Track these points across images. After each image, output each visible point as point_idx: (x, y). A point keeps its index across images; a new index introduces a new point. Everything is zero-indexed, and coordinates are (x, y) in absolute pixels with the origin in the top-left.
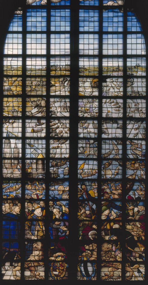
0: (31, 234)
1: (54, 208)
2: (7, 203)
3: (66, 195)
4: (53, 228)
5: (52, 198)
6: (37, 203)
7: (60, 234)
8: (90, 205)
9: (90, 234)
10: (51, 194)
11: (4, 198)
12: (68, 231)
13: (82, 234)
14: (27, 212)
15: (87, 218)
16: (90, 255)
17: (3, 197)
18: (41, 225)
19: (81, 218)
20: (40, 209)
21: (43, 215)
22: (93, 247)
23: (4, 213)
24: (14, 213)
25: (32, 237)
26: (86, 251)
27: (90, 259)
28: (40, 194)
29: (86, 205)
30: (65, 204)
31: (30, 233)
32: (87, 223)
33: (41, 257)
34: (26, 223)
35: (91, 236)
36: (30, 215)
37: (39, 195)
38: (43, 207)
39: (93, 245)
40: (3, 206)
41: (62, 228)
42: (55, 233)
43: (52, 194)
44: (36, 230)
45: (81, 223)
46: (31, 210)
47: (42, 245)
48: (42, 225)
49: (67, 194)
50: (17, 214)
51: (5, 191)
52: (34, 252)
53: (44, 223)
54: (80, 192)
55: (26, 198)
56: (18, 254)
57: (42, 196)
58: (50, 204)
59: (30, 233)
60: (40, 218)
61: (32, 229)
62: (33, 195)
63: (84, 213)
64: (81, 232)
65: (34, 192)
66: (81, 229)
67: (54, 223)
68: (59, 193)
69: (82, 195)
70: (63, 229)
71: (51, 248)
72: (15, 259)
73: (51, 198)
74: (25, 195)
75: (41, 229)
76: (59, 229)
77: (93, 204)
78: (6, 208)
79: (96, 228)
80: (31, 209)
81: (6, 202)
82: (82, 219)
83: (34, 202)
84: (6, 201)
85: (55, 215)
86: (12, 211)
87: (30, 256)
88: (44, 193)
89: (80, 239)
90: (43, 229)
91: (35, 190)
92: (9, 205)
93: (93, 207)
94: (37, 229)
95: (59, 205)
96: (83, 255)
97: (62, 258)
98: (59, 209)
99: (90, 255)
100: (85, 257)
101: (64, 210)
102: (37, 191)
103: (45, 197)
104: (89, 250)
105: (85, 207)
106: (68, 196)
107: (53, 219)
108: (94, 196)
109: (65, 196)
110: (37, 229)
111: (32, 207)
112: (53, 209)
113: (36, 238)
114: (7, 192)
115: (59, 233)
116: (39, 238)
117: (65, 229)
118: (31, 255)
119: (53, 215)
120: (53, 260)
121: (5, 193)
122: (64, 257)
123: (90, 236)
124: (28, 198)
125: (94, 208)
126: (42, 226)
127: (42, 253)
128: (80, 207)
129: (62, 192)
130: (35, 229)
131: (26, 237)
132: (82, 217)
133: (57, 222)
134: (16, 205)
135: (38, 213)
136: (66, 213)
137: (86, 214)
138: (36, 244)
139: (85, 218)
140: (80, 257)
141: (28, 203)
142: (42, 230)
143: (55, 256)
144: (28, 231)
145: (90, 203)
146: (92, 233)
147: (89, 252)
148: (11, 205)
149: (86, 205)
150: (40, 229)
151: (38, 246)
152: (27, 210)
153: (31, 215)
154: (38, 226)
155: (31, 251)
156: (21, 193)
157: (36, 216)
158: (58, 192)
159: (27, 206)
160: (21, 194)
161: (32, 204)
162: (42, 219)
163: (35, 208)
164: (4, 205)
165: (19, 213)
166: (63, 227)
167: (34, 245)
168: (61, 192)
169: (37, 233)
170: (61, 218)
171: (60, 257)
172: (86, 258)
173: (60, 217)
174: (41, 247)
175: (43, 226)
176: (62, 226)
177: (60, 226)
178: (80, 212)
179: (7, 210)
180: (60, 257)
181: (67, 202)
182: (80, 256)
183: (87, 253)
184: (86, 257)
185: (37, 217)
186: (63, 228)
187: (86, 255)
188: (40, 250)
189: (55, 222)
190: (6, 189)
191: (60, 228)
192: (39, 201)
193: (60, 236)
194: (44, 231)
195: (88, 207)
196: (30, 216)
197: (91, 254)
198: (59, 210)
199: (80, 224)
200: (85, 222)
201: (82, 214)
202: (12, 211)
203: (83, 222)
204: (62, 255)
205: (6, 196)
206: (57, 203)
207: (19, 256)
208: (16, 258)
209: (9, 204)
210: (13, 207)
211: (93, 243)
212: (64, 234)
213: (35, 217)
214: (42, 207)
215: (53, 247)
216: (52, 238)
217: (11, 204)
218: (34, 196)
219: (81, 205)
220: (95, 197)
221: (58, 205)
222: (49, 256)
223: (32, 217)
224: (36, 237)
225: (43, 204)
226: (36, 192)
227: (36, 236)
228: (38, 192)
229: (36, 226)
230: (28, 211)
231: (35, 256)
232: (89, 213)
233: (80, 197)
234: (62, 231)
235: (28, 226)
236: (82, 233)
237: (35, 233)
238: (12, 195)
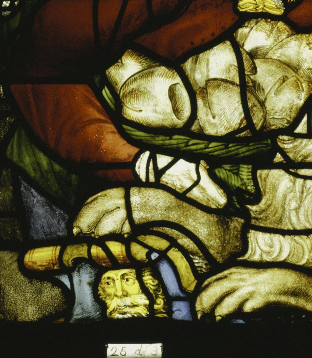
39: (253, 55)
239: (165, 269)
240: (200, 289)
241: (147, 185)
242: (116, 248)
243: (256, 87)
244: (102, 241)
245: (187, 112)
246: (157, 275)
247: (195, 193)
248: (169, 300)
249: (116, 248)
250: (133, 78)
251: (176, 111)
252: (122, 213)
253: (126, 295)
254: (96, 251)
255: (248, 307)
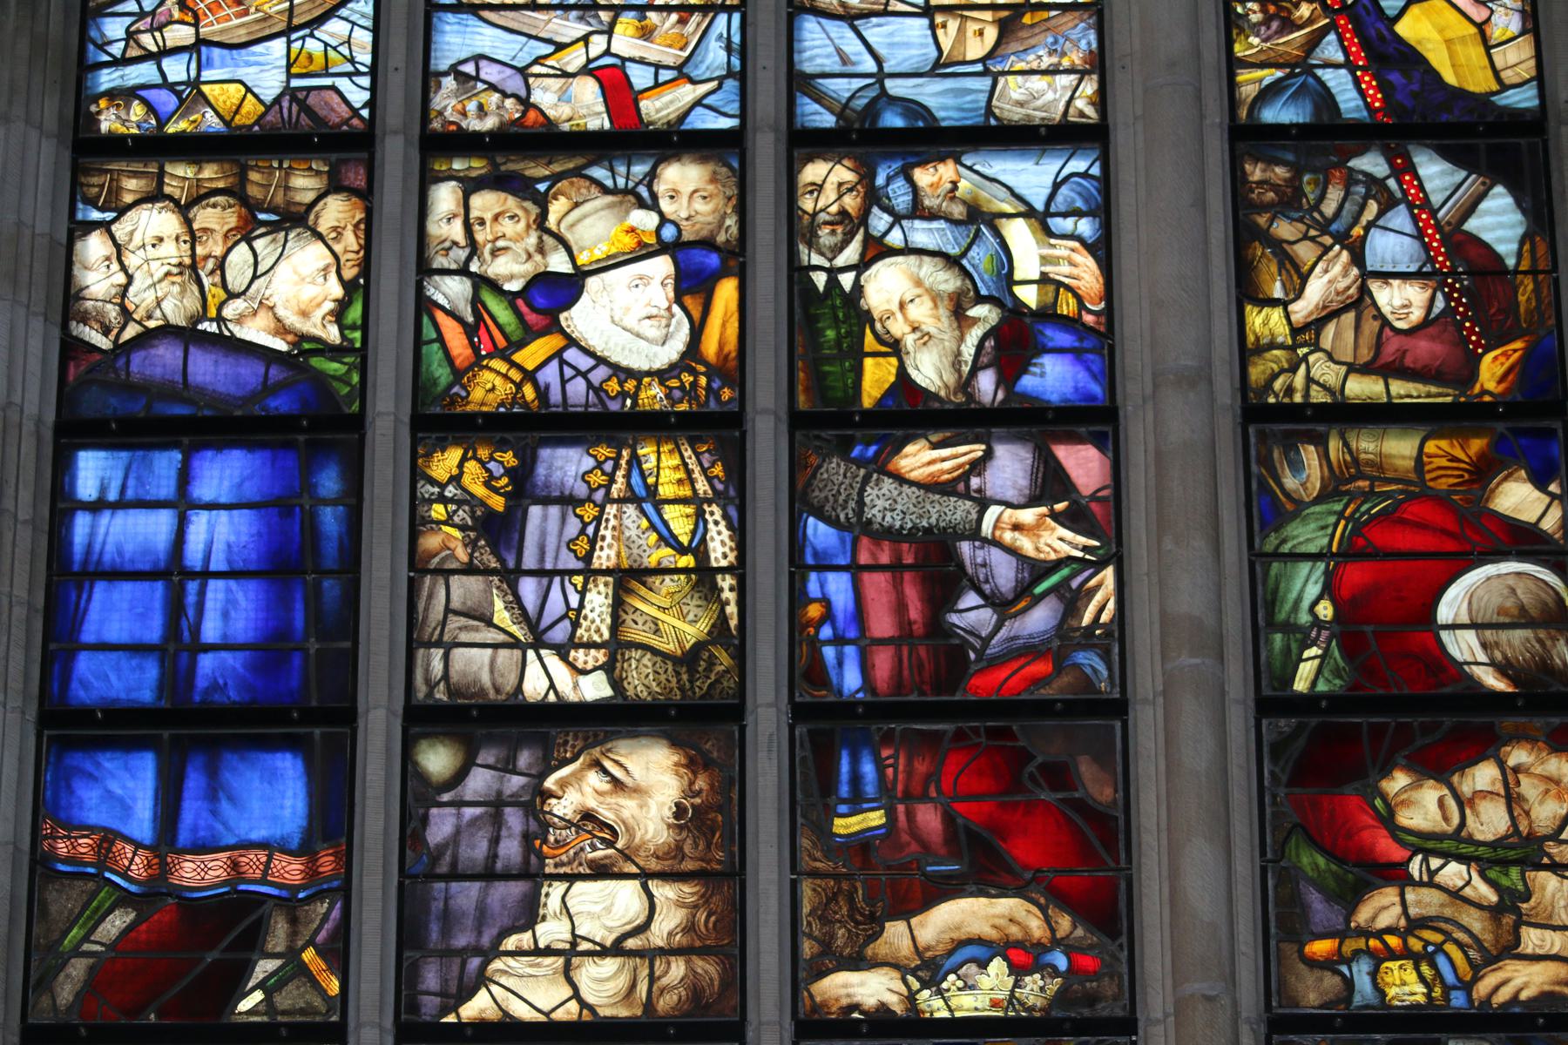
0: (518, 631)
1: (877, 250)
2: (155, 196)
3: (1053, 71)
4: (860, 528)
5: (842, 110)
6: (605, 190)
7: (971, 614)
8: (1436, 199)
9: (1452, 605)
10: (833, 64)
11: (104, 127)
12: (1099, 566)
13: (1325, 610)
14: (451, 314)
15: (1399, 388)
16: (1475, 921)
17: (94, 120)
18: (666, 491)
19: (1299, 380)
20: (662, 266)
21: (710, 347)
22: (1512, 799)
23: (104, 343)
24: (256, 332)
25: (533, 667)
26: (1415, 867)
27: (1483, 988)
28: (658, 67)
29: (1373, 207)
30: (1051, 198)
31: (502, 616)
32: (1400, 448)
33: (677, 970)
34: (445, 463)
35: (1470, 637)
36: (496, 353)
37: (640, 77)
38: (707, 243)
39: (1516, 770)
40: (95, 247)
41: (1008, 536)
42: (900, 607)
43: (844, 59)
44: (590, 573)
45: (1310, 454)
46: (514, 286)
47: (689, 792)
48: (686, 491)
49: (1075, 58)
50: (294, 344)
51: (131, 36)
52: (558, 889)
53: (718, 470)
54: (1266, 22)
55: (436, 125)
56: (293, 934)
57: (686, 94)
58: (807, 204)
59: (502, 616)
60: (653, 396)
61: (529, 561)
62: (556, 83)
63: (1349, 318)
64: (1313, 590)
65: (560, 47)
66: (1308, 534)
67: (881, 467)
68: (946, 44)
69: (1301, 66)
70: (1026, 545)
71: (845, 825)
72: (245, 1005)
73: (827, 120)
74: (429, 79)
75: (682, 550)
76: (965, 548)
77: (1473, 183)
78: (132, 261)
79: (1550, 523)
80: (511, 270)
81: (131, 184)
82: (1318, 396)
83: (577, 173)
84: (135, 175)
85: (895, 347)
86: (228, 312)
87: (495, 952)
88: (715, 56)
89: (1301, 685)
90: (699, 549)
91: (581, 19)
92: (188, 222)
93: (1472, 225)
94: (604, 557)
95: (958, 211)
96: (1366, 933)
97: (1018, 971)
98: (952, 262)
99: (1475, 921)
100: (1406, 954)
101: (1036, 276)
102: (610, 32)
103: (734, 108)
104: (1455, 845)
105: (1357, 231)
106: (1089, 87)
107: (867, 403)
108: (1479, 82)
109: (1037, 83)
110: (604, 557)
111: (541, 249)
112: (862, 266)
113: (595, 688)
114: (158, 56)
115: (971, 599)
116: (642, 678)
117: (1059, 541)
118: (510, 943)
119: (859, 354)
120: (883, 1007)
121: (123, 62)
122: (1061, 962)
123: (1463, 646)
124: (474, 125)
125: (1487, 237)
126: (695, 500)
127: (695, 907)
128: (1284, 229)
129: (991, 34)
130: (588, 558)
131: (437, 666)
132: (1326, 372)
133: (935, 446)
134: (295, 219)
135: (630, 322)
136: (1067, 306)
137: (1370, 327)
138: (594, 779)
139: (1362, 388)
140: (1313, 963)
141: (471, 186)
142: (687, 561)
143: (904, 947)
144: (464, 589)
145: (1435, 173)
146: (1496, 601)
147: (1453, 873)
148: (215, 218)
149: (1373, 207)
150: (664, 555)
151: (628, 806)
152: (451, 291)
153: (518, 357)
154: (630, 510)
155: (516, 889)
156: (365, 58)
157: (601, 360)
158: (933, 27)
159: (456, 231)
160: (373, 71)
161: (543, 202)
162: (683, 407)
163: (582, 259)
164: (106, 226)
165: (332, 334)
166: (1028, 516)
167: (563, 784)
168: (972, 27)
169: (618, 606)
170: (986, 383)
171: (997, 966)
172: (1411, 976)
173: (976, 368)
174: (680, 811)
175: (714, 513)
176: (1009, 505)
177: (983, 503)
178: (1284, 304)
179: (141, 297)
180: (983, 965)
181: (1078, 165)
182: (1321, 947)
183: (1423, 901)
184: (1416, 959)
185: (613, 386)
186: (1017, 527)
187: (1416, 925)
188: (654, 865)
189: (898, 448)
190: (142, 15)
191: (974, 534)
192: (639, 169)
193: (980, 654)
194: (726, 582)
195: (1408, 227)
196: (498, 364)
197: (1495, 912)
198: (948, 282)
199: (1297, 466)
200: (1366, 444)
201: (1317, 324)
202: (228, 312)
203: (1334, 445)
204: (1014, 931)
205: (137, 111)
206: (923, 177)
207: (309, 955)
208: (258, 996)
209: (184, 210)
210: (243, 247)
211: (1520, 737)
212: (1039, 619)
213: (577, 388)
214: (687, 236)
215: (876, 818)
216: (851, 679)
217: (205, 217)
218: (563, 96)
219: (1289, 202)
220: (1504, 87)
221: (932, 216)
222: (808, 948)
223: (530, 376)
224: (600, 676)
225: (700, 206)
226: (598, 44)
227: (601, 656)
228: (625, 42)
229: (589, 512)
230: (476, 302)
231: (571, 953)
232: (1417, 315)
233: (1268, 93)
234: (1004, 573)
235: (462, 515)
236: (1329, 590)
237: (575, 616)
238: (233, 87)
239: (1441, 961)
240: (1476, 979)
241: (1421, 884)
242: (1393, 941)
243: (1521, 798)
244: (1379, 934)
245: (1456, 820)
246: (1433, 965)
247: (1468, 892)
248: (1447, 989)
249: (1393, 941)
250: (1404, 790)
251: (1446, 819)
252: (1398, 909)
253: (1404, 984)
254: (1373, 943)
255: (1524, 996)
